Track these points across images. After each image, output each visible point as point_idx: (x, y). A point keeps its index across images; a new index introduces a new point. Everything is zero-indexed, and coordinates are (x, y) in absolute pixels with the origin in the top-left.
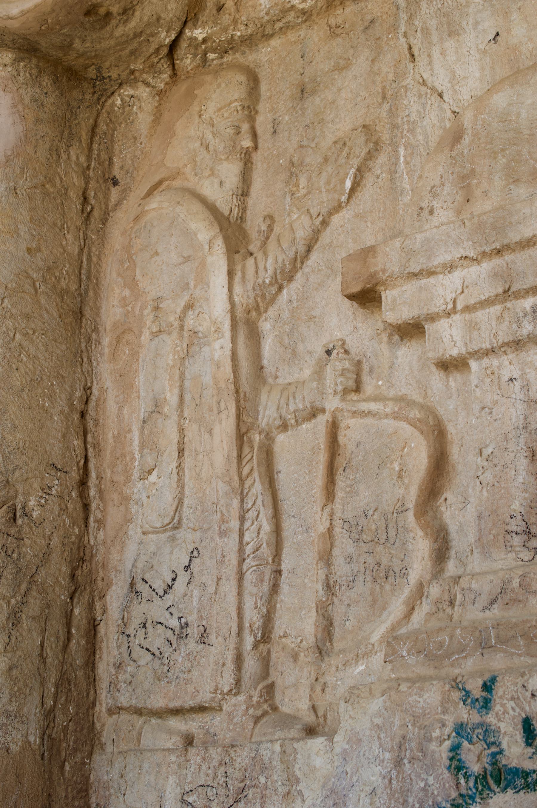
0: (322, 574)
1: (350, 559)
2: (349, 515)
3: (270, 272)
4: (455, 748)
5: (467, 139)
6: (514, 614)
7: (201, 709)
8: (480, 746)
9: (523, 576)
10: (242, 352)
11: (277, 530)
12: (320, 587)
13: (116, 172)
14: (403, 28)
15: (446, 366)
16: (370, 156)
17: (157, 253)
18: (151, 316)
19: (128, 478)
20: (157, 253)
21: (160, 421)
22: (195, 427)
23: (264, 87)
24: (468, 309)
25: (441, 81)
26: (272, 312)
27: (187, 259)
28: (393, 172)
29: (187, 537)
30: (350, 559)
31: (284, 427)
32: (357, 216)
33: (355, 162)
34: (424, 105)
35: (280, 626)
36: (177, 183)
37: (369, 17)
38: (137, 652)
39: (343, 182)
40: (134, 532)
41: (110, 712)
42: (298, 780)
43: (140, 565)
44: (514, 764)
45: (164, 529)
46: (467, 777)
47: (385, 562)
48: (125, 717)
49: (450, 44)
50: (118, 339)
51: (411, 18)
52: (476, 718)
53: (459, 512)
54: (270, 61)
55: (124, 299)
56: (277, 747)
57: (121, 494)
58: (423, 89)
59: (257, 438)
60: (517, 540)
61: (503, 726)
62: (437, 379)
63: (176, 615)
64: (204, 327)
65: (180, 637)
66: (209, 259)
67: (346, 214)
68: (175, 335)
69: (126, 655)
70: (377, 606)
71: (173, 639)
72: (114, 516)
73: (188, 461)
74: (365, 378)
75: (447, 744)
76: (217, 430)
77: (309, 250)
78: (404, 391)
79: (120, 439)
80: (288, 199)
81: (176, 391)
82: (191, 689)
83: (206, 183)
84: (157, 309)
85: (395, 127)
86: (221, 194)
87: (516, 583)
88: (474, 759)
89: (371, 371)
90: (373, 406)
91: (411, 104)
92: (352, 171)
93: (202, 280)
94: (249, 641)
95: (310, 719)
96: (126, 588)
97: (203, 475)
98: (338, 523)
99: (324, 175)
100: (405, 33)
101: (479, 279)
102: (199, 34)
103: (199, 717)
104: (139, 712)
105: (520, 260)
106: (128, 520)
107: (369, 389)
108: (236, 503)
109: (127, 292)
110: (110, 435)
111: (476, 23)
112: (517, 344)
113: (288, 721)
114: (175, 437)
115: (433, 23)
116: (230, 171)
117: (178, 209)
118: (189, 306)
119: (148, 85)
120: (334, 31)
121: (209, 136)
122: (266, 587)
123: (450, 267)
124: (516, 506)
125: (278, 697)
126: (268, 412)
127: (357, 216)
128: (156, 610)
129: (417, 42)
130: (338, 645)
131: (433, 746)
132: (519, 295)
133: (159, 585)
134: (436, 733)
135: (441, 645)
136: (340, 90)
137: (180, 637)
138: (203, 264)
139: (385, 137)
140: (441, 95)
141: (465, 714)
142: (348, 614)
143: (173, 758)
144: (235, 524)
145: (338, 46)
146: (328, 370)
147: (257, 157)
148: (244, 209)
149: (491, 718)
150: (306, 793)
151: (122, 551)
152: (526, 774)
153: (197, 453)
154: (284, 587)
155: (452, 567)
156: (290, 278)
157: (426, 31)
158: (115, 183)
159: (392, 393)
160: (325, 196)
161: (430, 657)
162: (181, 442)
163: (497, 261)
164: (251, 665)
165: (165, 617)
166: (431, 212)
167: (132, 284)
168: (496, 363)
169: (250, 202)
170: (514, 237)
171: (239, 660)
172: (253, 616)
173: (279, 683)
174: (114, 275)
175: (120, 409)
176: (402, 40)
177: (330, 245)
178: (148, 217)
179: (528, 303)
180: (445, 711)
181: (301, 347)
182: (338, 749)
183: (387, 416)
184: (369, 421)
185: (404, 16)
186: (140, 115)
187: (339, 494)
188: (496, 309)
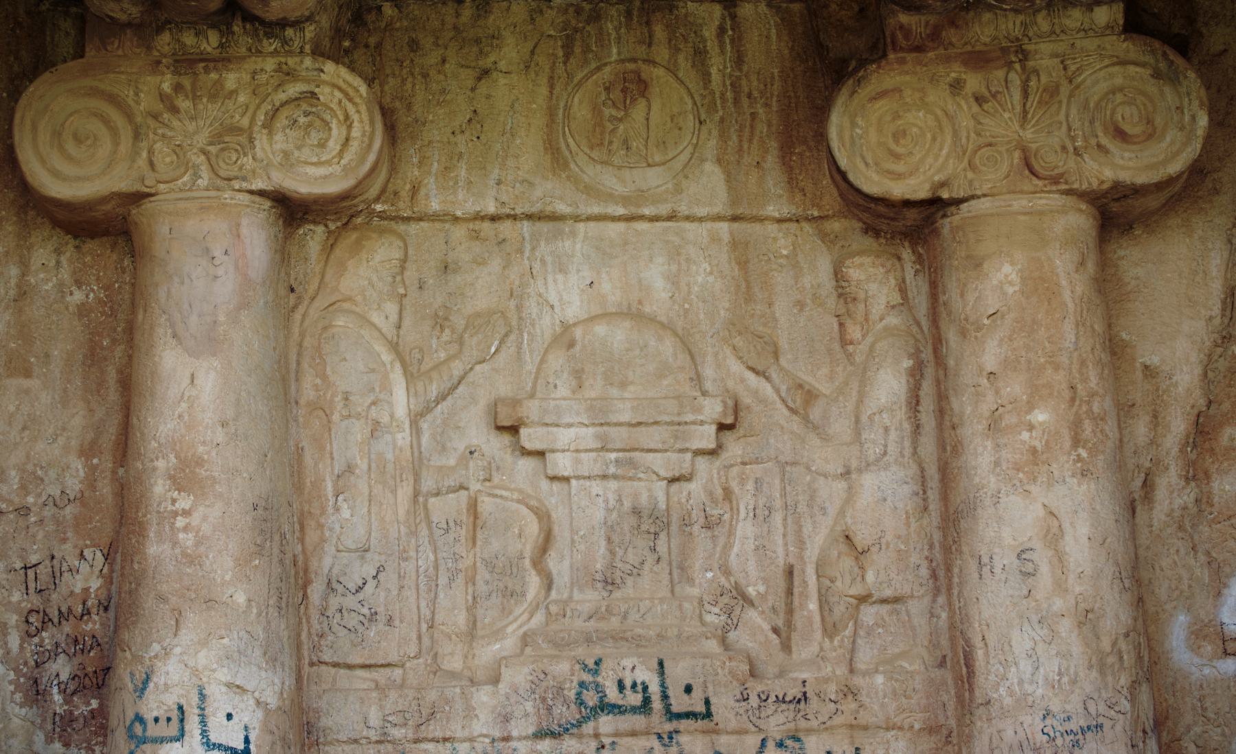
0: (470, 590)
1: (487, 583)
2: (486, 556)
3: (435, 394)
4: (579, 694)
5: (578, 348)
6: (602, 625)
7: (388, 665)
8: (591, 693)
9: (608, 606)
10: (415, 445)
11: (436, 560)
12: (470, 598)
13: (292, 282)
14: (527, 254)
15: (554, 478)
16: (506, 335)
17: (345, 359)
18: (341, 404)
19: (323, 512)
20: (345, 359)
21: (352, 478)
22: (380, 487)
23: (410, 252)
24: (577, 451)
25: (553, 297)
26: (429, 417)
27: (373, 371)
28: (519, 348)
29: (374, 560)
30: (487, 583)
31: (437, 494)
32: (493, 369)
33: (498, 336)
34: (541, 311)
35: (439, 618)
36: (346, 305)
37: (502, 236)
38: (335, 628)
39: (490, 348)
40: (330, 549)
41: (312, 664)
42: (474, 709)
43: (335, 571)
44: (613, 702)
45: (356, 550)
46: (586, 708)
47: (510, 585)
48: (323, 667)
49: (560, 277)
50: (310, 413)
51: (533, 249)
52: (591, 679)
53: (559, 565)
54: (416, 235)
55: (316, 385)
56: (458, 690)
57: (318, 522)
58: (541, 300)
59: (421, 499)
60: (599, 585)
61: (607, 683)
62: (545, 484)
63: (367, 606)
64: (386, 419)
65: (370, 620)
66: (391, 376)
67: (485, 367)
68: (363, 420)
69: (326, 629)
70: (505, 611)
71: (366, 622)
72: (312, 536)
73: (374, 509)
74: (494, 473)
75: (573, 691)
76: (400, 492)
77: (460, 382)
78: (522, 486)
79: (318, 484)
80: (434, 341)
81: (366, 461)
82: (381, 653)
83: (375, 314)
84: (347, 399)
85: (520, 318)
86: (387, 328)
87: (603, 609)
88: (591, 699)
89: (498, 469)
90: (504, 493)
91: (532, 307)
92: (496, 343)
93: (387, 387)
94: (424, 626)
95: (467, 673)
96: (324, 587)
97: (387, 519)
98: (478, 559)
99: (475, 338)
100: (528, 258)
101: (587, 436)
102: (379, 207)
103: (382, 670)
104: (336, 665)
105: (613, 431)
106: (323, 540)
107: (496, 480)
108: (413, 541)
109: (318, 381)
110: (308, 480)
111: (578, 271)
112: (604, 477)
113: (453, 675)
114: (366, 491)
115: (549, 259)
116: (391, 308)
117: (363, 332)
118: (374, 403)
119: (326, 226)
120: (476, 236)
121: (375, 279)
122: (433, 594)
123: (570, 425)
124: (598, 566)
125: (439, 661)
126: (428, 484)
127: (493, 369)
128: (350, 601)
129: (537, 266)
130: (480, 633)
131: (566, 692)
132: (607, 450)
133: (352, 586)
134: (568, 686)
135: (563, 639)
136: (477, 278)
137: (370, 620)
138: (386, 376)
139: (514, 323)
140: (552, 307)
141: (587, 678)
142: (487, 615)
143: (374, 694)
144: (412, 554)
145: (477, 247)
146: (471, 464)
147: (406, 301)
148: (398, 336)
149: (599, 679)
150: (481, 716)
151: (320, 560)
152: (620, 707)
153: (382, 504)
154: (441, 595)
155: (554, 594)
156: (444, 398)
157: (543, 261)
158: (292, 290)
159: (513, 486)
160: (475, 353)
161: (556, 645)
162: (370, 495)
163: (598, 428)
164: (426, 641)
165: (358, 607)
166: (555, 387)
167: (324, 377)
168: (588, 483)
169: (401, 333)
170: (613, 418)
171: (419, 638)
172: (425, 612)
173: (440, 651)
174: (306, 366)
175: (316, 464)
176: (526, 262)
177: (473, 383)
178: (334, 330)
179: (613, 456)
180: (573, 675)
181: (449, 445)
182: (502, 692)
183: (512, 500)
184: (498, 500)
185: (528, 247)
186: (311, 243)
187: (479, 543)
188: (594, 454)
